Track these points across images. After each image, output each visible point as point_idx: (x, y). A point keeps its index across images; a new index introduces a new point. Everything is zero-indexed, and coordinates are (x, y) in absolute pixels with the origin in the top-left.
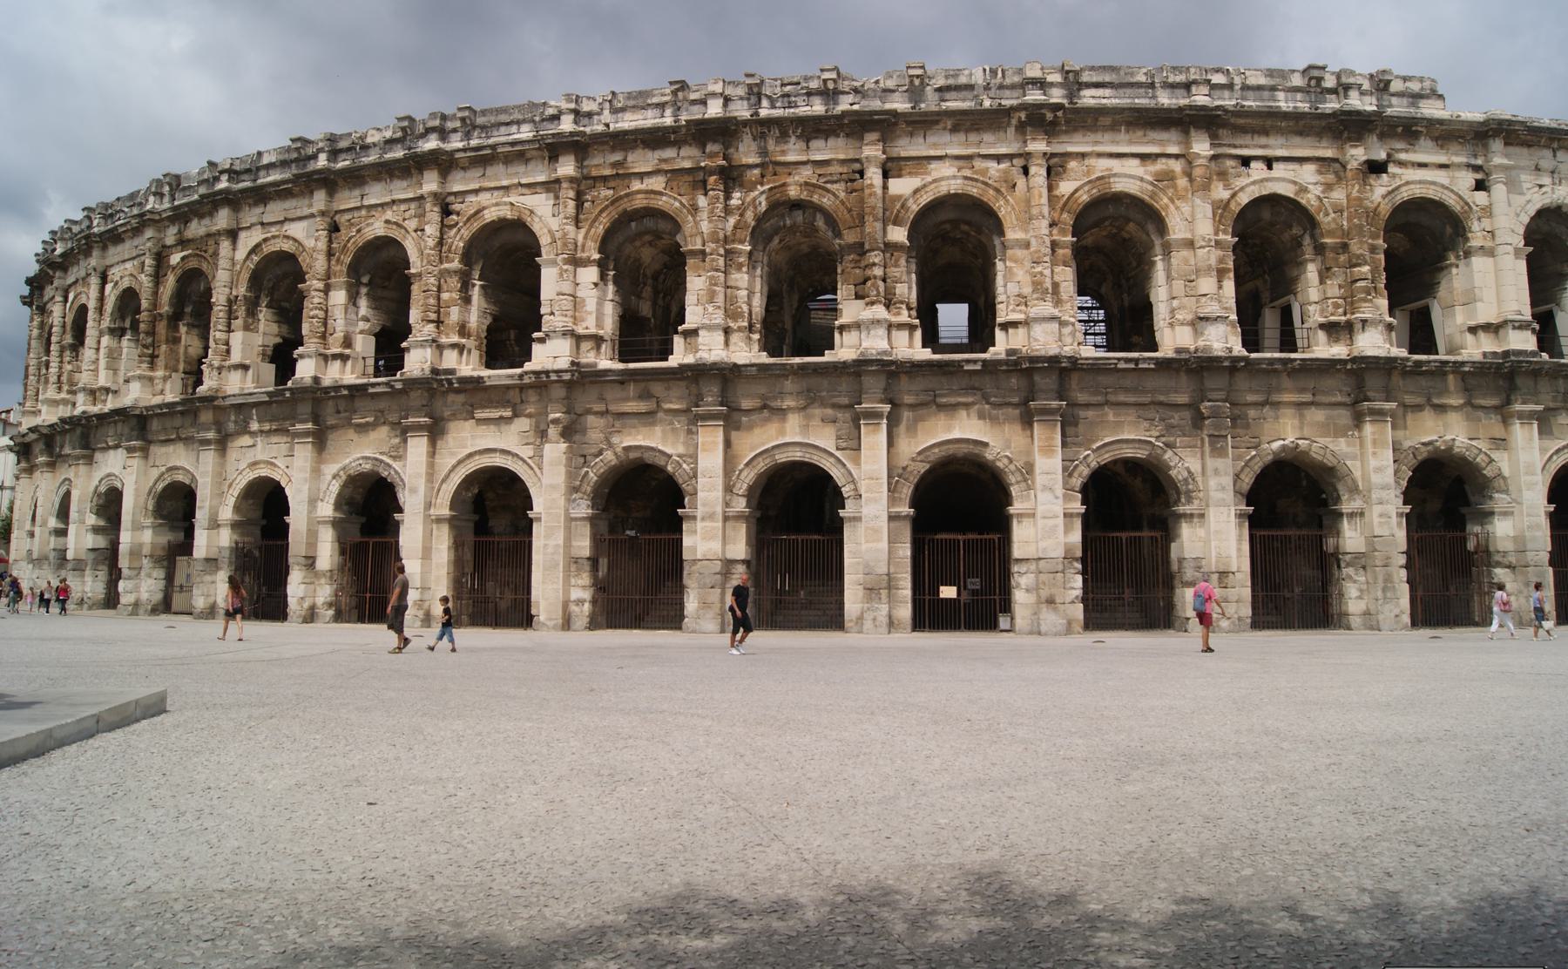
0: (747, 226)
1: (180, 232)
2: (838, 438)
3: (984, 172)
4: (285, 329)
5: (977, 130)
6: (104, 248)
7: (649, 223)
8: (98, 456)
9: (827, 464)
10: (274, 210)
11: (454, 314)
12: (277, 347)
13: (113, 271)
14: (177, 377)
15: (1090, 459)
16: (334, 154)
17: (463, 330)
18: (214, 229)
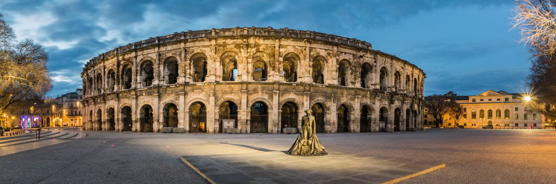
7: (229, 54)
9: (266, 102)
11: (188, 71)
15: (313, 102)
17: (190, 75)
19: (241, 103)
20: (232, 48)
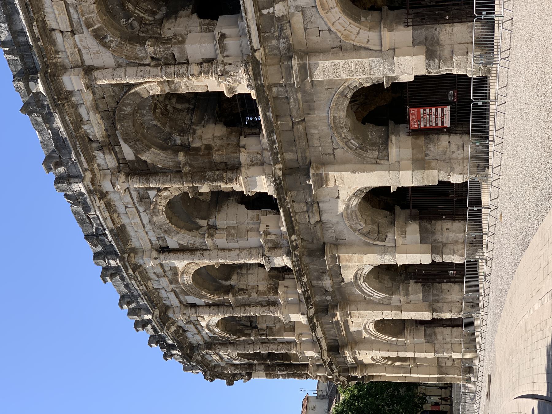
1: (101, 149)
4: (183, 13)
6: (134, 250)
12: (200, 17)
13: (154, 240)
14: (243, 141)
18: (87, 98)
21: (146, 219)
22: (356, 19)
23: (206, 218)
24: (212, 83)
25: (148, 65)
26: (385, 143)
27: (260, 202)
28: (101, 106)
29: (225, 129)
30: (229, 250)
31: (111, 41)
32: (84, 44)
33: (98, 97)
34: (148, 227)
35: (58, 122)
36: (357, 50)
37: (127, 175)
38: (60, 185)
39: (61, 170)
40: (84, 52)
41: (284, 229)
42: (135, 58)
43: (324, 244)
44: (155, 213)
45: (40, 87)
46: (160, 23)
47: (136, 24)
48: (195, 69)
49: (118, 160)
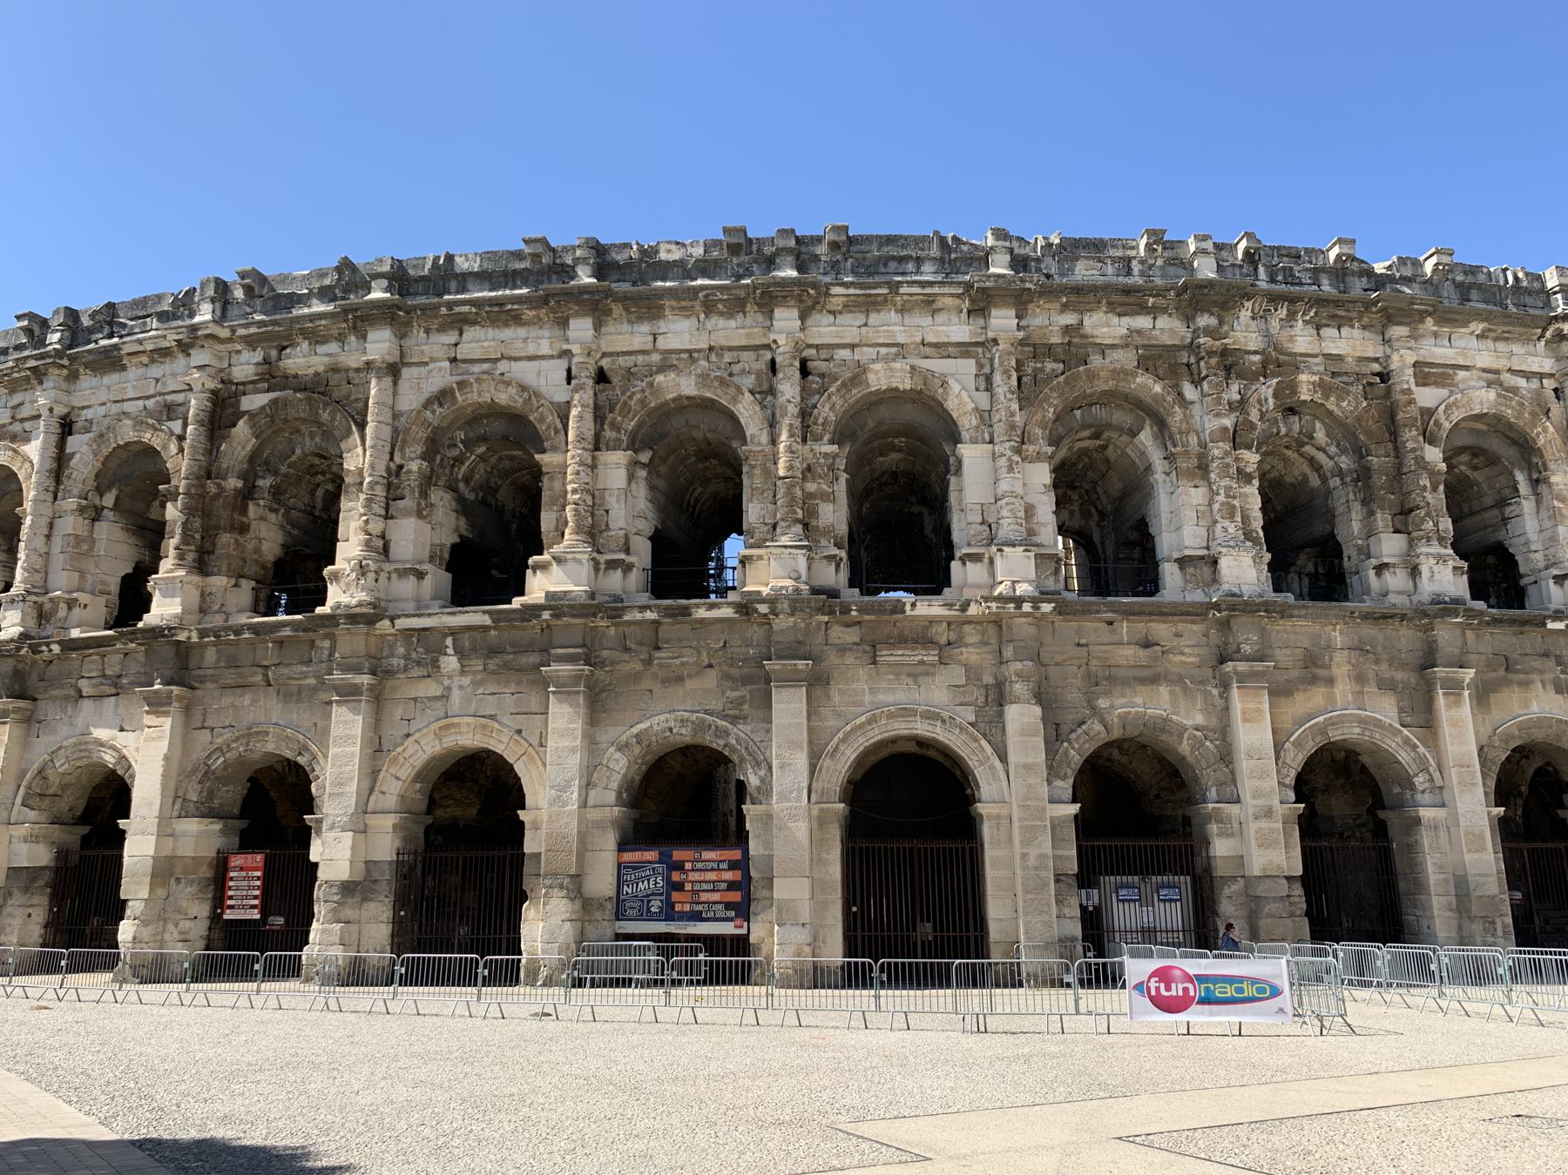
0: (1253, 426)
1: (266, 361)
2: (1401, 710)
3: (1515, 390)
4: (463, 522)
5: (1506, 339)
6: (73, 377)
8: (49, 709)
9: (1391, 744)
10: (478, 341)
12: (454, 546)
13: (88, 414)
14: (247, 585)
16: (600, 272)
18: (353, 360)
19: (1226, 756)
20: (1121, 373)
21: (127, 407)
22: (419, 777)
23: (116, 507)
24: (350, 549)
25: (392, 459)
26: (207, 811)
27: (133, 598)
28: (336, 376)
29: (271, 558)
30: (48, 537)
31: (434, 412)
32: (435, 373)
33: (352, 374)
34: (115, 408)
35: (318, 307)
36: (372, 775)
37: (214, 393)
38: (212, 286)
39: (239, 294)
40: (422, 370)
41: (75, 633)
42: (404, 442)
43: (35, 700)
44: (139, 423)
45: (377, 294)
46: (452, 487)
47: (454, 453)
48: (377, 526)
49: (243, 384)
